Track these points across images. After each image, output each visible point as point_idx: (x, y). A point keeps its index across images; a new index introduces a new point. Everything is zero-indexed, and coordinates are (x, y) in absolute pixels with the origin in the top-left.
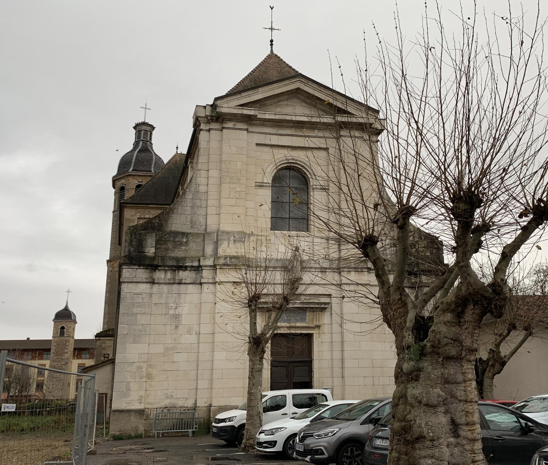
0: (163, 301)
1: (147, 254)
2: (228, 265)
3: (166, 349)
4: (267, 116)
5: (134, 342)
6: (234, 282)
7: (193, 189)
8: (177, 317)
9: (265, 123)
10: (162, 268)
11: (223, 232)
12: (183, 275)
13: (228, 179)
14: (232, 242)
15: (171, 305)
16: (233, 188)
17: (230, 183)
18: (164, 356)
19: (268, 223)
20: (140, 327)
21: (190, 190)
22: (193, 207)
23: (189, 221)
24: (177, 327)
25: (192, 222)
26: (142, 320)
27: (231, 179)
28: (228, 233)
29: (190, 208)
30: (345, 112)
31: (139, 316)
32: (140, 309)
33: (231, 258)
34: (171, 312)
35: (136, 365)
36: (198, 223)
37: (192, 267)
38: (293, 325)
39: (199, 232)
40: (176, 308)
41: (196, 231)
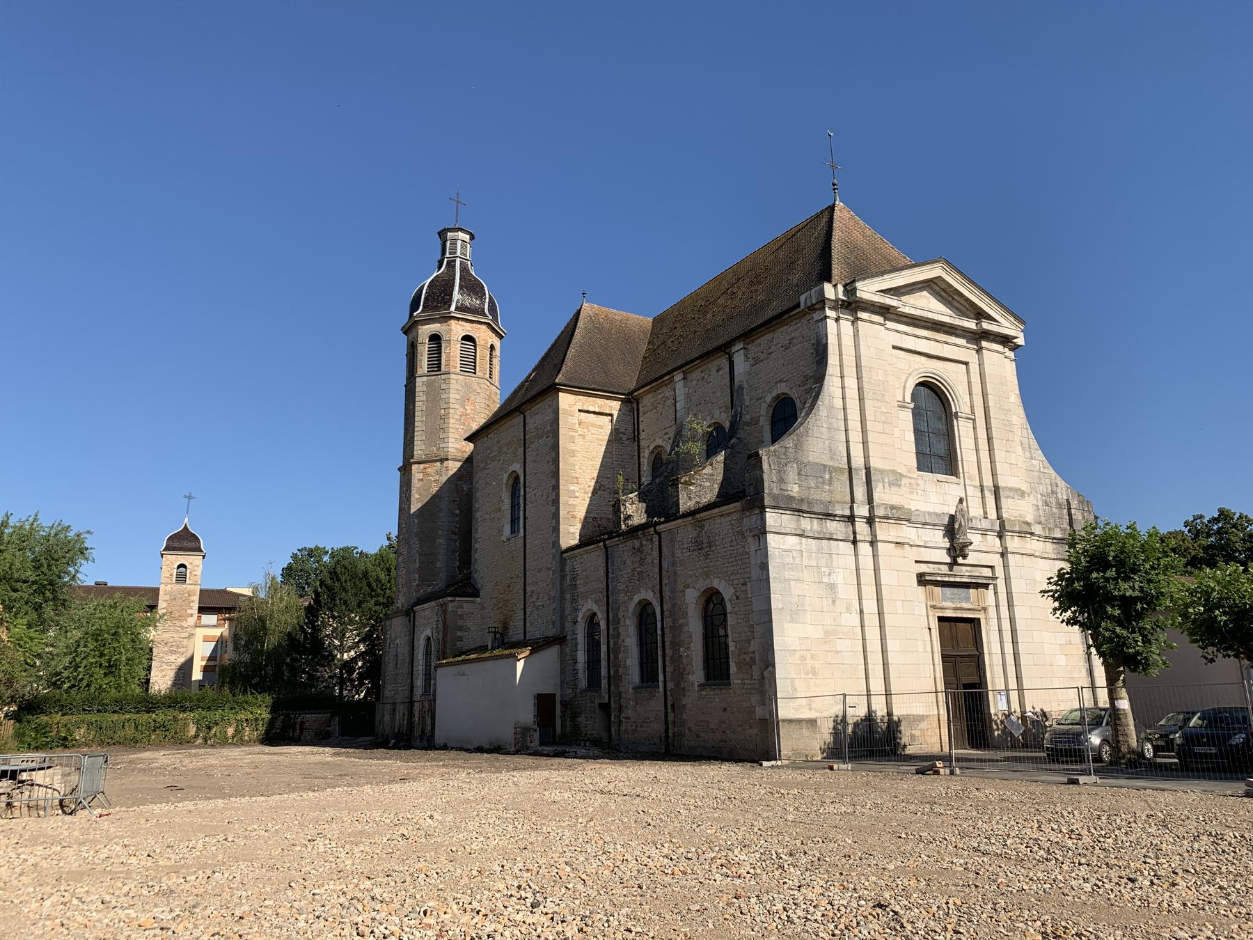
0: (813, 563)
1: (790, 493)
2: (888, 518)
3: (826, 632)
4: (907, 310)
5: (793, 621)
6: (897, 543)
7: (826, 402)
8: (832, 587)
9: (902, 319)
10: (808, 515)
11: (876, 470)
12: (835, 527)
13: (871, 394)
14: (887, 485)
15: (824, 569)
16: (879, 408)
17: (874, 400)
18: (826, 642)
19: (913, 462)
20: (796, 600)
21: (823, 404)
22: (829, 429)
23: (827, 448)
24: (834, 602)
25: (830, 451)
26: (796, 588)
27: (874, 393)
28: (881, 471)
29: (826, 430)
30: (989, 318)
31: (792, 583)
32: (792, 573)
33: (893, 507)
34: (825, 580)
35: (798, 652)
36: (837, 453)
37: (843, 516)
38: (959, 605)
39: (841, 466)
40: (830, 574)
41: (837, 465)
